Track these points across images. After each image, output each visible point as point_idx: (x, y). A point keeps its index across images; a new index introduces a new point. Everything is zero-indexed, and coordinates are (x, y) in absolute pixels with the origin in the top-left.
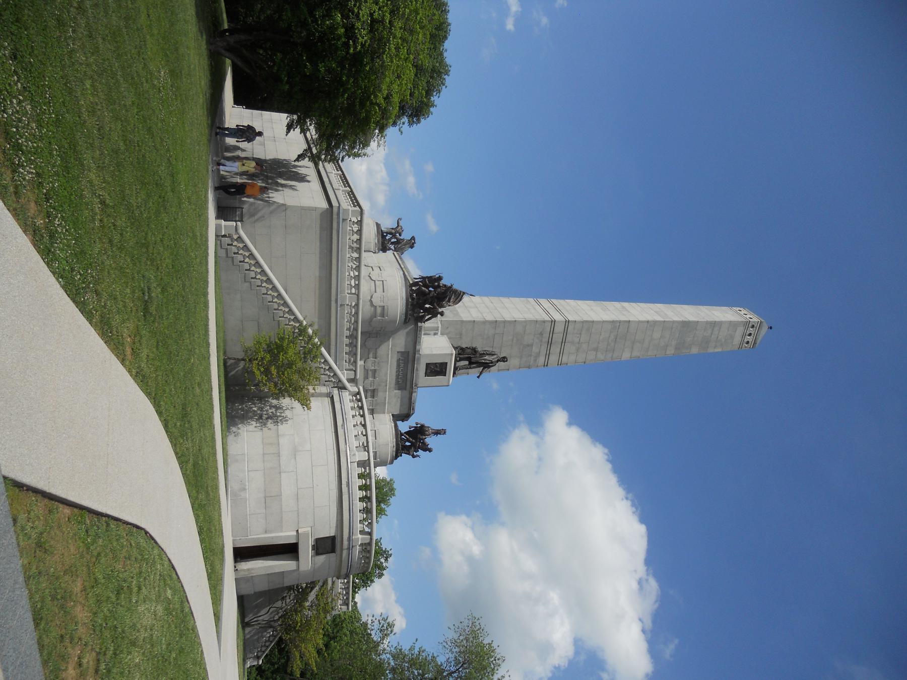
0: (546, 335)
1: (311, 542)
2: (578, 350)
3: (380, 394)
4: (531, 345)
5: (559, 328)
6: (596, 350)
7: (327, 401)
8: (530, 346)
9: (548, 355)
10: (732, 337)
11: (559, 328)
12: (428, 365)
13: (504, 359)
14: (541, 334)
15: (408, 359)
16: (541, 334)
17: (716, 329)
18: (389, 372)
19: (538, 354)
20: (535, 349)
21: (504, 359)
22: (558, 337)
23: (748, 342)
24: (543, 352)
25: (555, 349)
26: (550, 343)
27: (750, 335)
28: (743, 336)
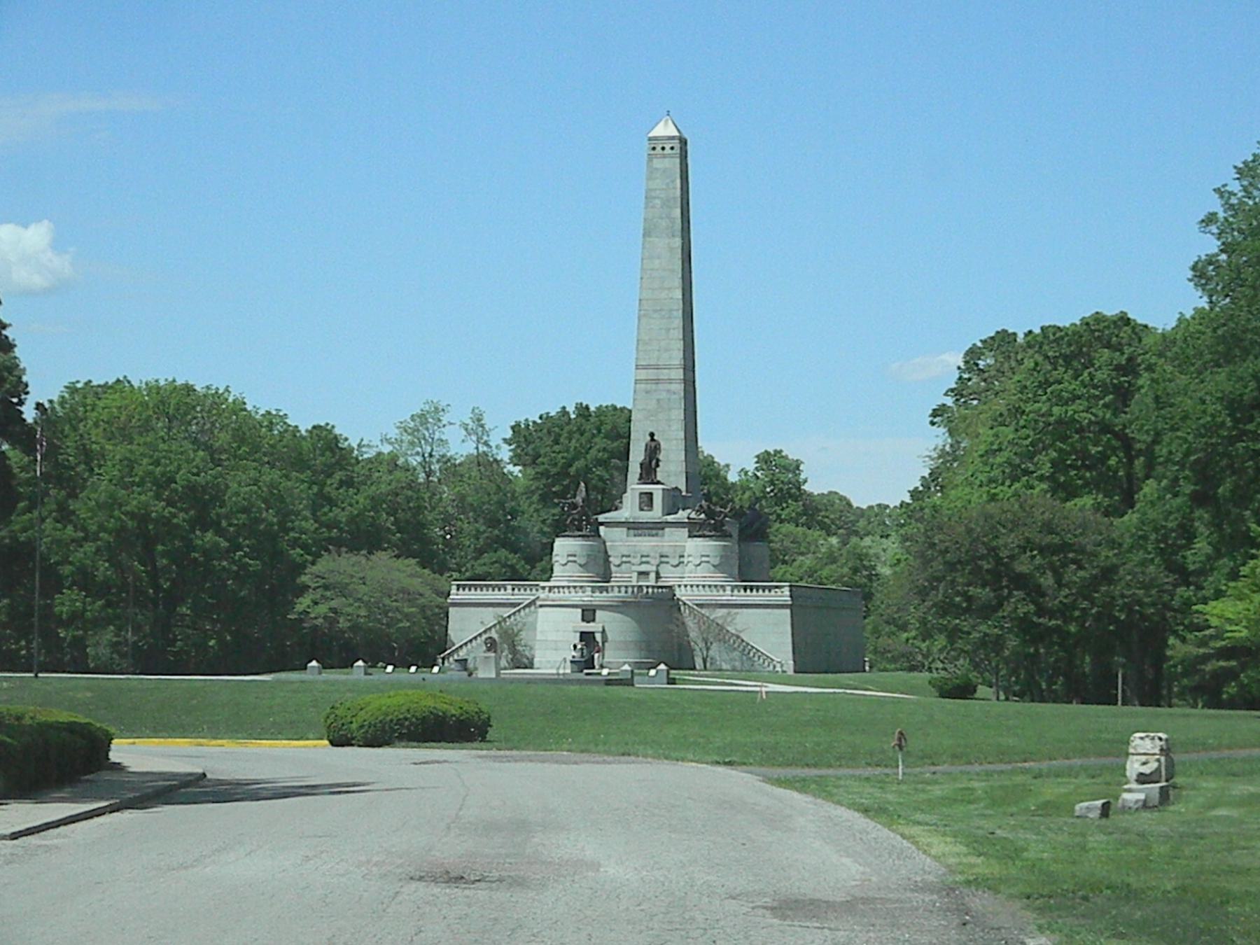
0: (649, 387)
1: (584, 624)
2: (666, 350)
3: (665, 551)
4: (658, 400)
5: (643, 374)
6: (668, 330)
7: (541, 610)
8: (658, 400)
9: (670, 381)
10: (665, 171)
11: (643, 374)
12: (641, 509)
13: (652, 435)
14: (647, 392)
15: (634, 527)
16: (647, 392)
17: (653, 194)
18: (646, 543)
19: (668, 391)
20: (664, 395)
21: (652, 435)
22: (651, 374)
23: (672, 148)
24: (668, 386)
25: (664, 374)
26: (657, 381)
27: (663, 148)
28: (664, 156)
